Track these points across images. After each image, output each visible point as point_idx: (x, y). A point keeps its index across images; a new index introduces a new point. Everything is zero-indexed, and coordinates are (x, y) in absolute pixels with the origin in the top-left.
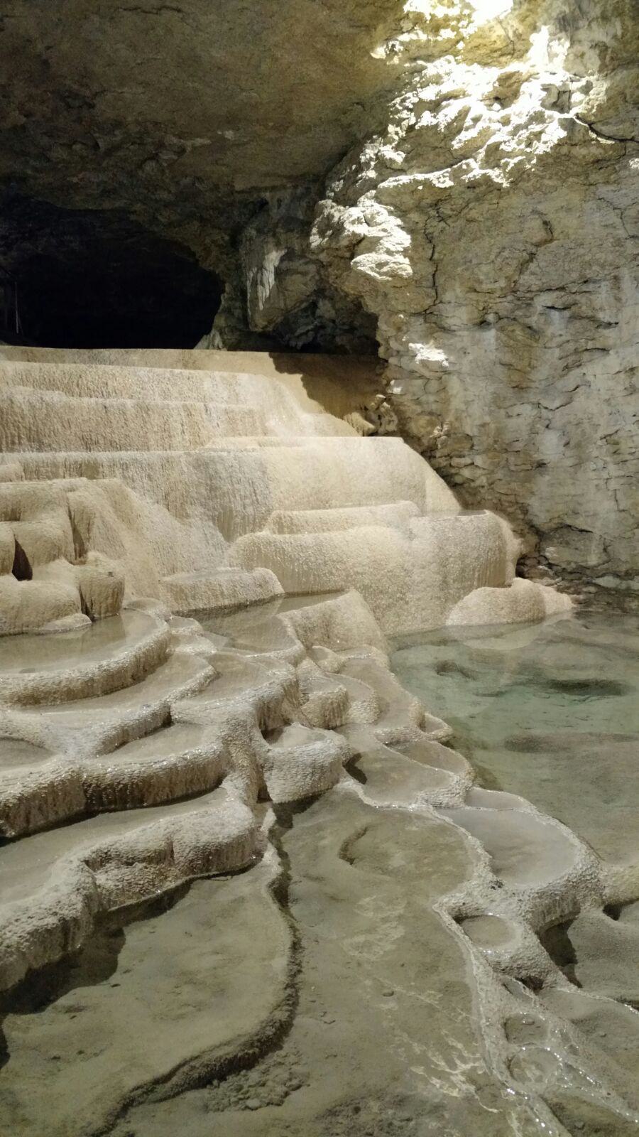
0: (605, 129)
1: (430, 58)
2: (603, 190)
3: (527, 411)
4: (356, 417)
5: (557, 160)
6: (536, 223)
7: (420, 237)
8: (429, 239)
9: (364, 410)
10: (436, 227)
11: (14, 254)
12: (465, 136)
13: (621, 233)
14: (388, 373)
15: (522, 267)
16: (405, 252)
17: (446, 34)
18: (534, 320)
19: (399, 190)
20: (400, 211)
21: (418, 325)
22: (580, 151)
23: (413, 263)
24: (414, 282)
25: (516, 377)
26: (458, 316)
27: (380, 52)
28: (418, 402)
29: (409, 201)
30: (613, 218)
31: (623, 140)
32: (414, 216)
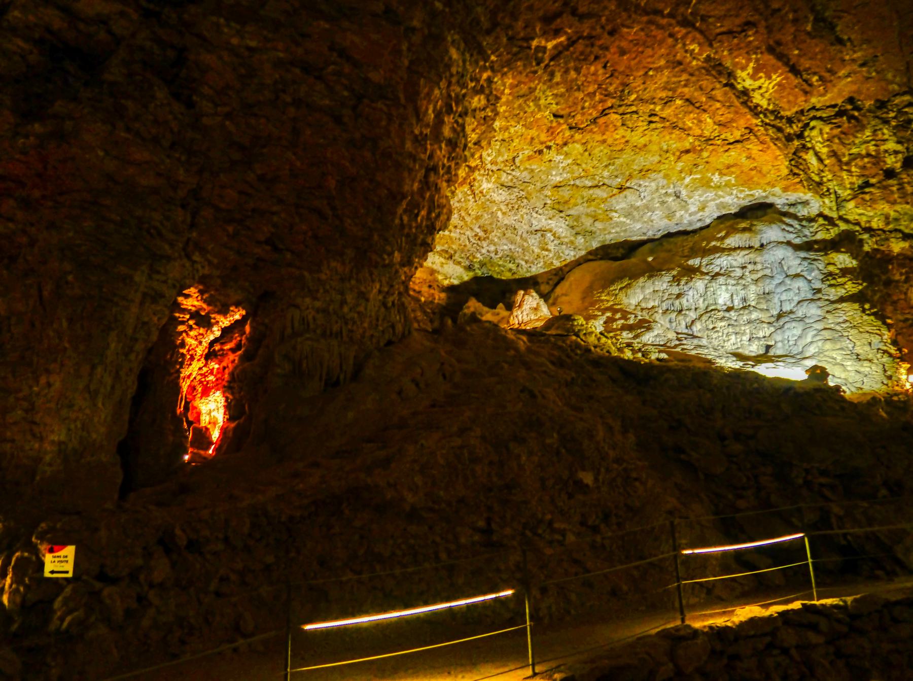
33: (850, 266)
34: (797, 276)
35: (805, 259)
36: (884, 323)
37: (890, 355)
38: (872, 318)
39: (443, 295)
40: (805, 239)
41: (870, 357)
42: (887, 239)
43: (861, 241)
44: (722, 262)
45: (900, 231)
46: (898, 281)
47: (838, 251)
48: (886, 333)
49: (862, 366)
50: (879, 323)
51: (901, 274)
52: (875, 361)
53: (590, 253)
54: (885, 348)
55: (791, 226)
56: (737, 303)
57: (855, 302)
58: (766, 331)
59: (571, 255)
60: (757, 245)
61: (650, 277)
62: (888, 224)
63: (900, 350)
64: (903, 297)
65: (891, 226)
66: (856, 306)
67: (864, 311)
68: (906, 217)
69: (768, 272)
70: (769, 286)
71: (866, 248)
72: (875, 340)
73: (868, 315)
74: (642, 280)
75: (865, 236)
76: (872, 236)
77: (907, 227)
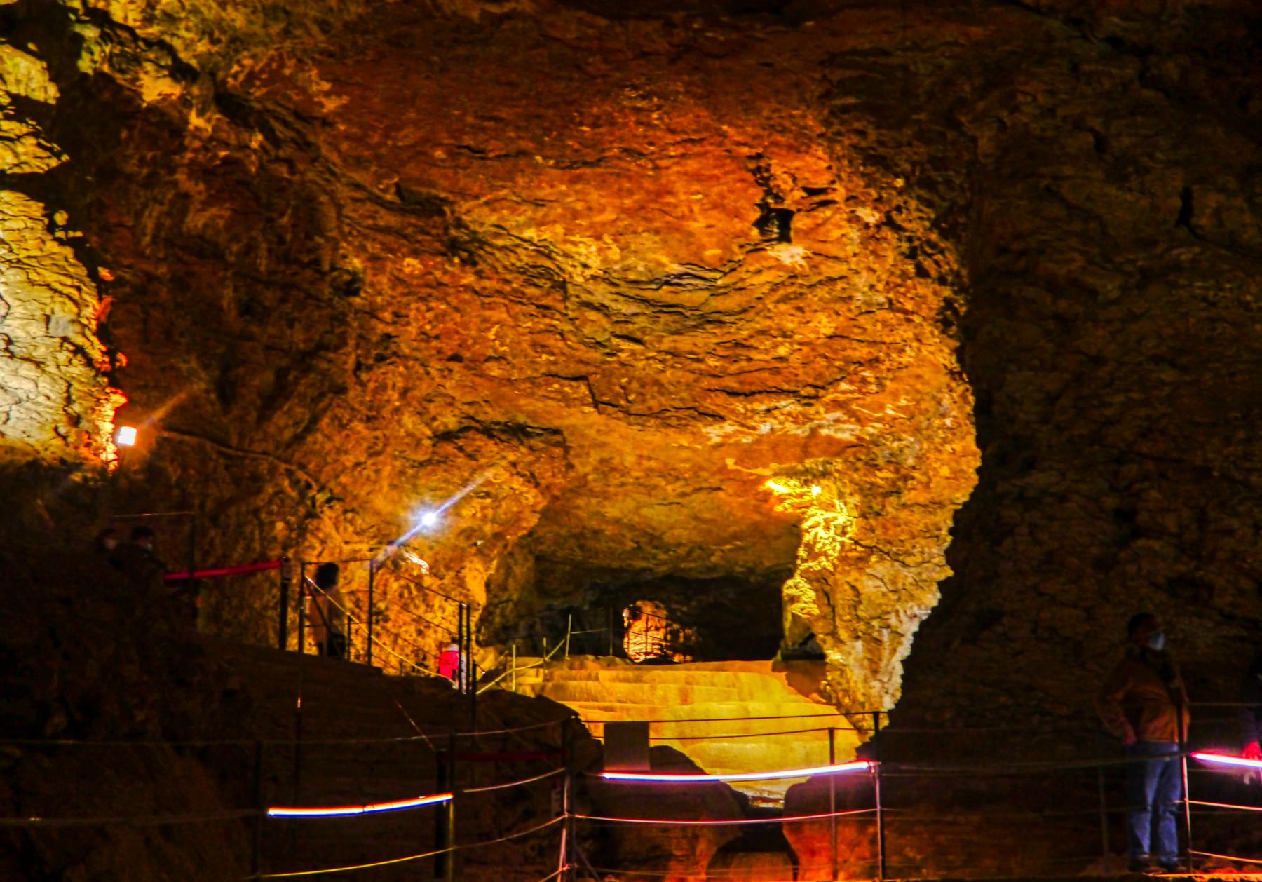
0: (863, 543)
1: (807, 507)
2: (868, 571)
3: (876, 684)
4: (815, 696)
5: (843, 559)
6: (847, 587)
7: (821, 594)
8: (827, 595)
9: (822, 693)
10: (827, 588)
11: (693, 603)
12: (819, 546)
13: (884, 589)
14: (828, 667)
15: (855, 608)
16: (814, 602)
17: (806, 498)
18: (875, 634)
19: (807, 571)
20: (809, 581)
21: (829, 639)
22: (850, 554)
23: (819, 607)
24: (823, 617)
25: (874, 666)
26: (843, 634)
27: (779, 508)
28: (839, 684)
29: (812, 577)
30: (879, 583)
31: (871, 548)
32: (816, 584)
33: (39, 96)
36: (93, 275)
37: (89, 362)
38: (68, 251)
41: (39, 353)
42: (137, 60)
43: (80, 39)
45: (170, 50)
46: (130, 178)
47: (20, 46)
48: (94, 302)
49: (15, 373)
50: (82, 271)
51: (142, 161)
52: (52, 369)
54: (80, 340)
57: (34, 195)
62: (148, 20)
63: (110, 353)
64: (129, 221)
65: (154, 30)
66: (36, 208)
67: (51, 228)
68: (193, 20)
71: (85, 65)
72: (63, 312)
73: (61, 242)
75: (90, 32)
76: (105, 38)
77: (188, 45)
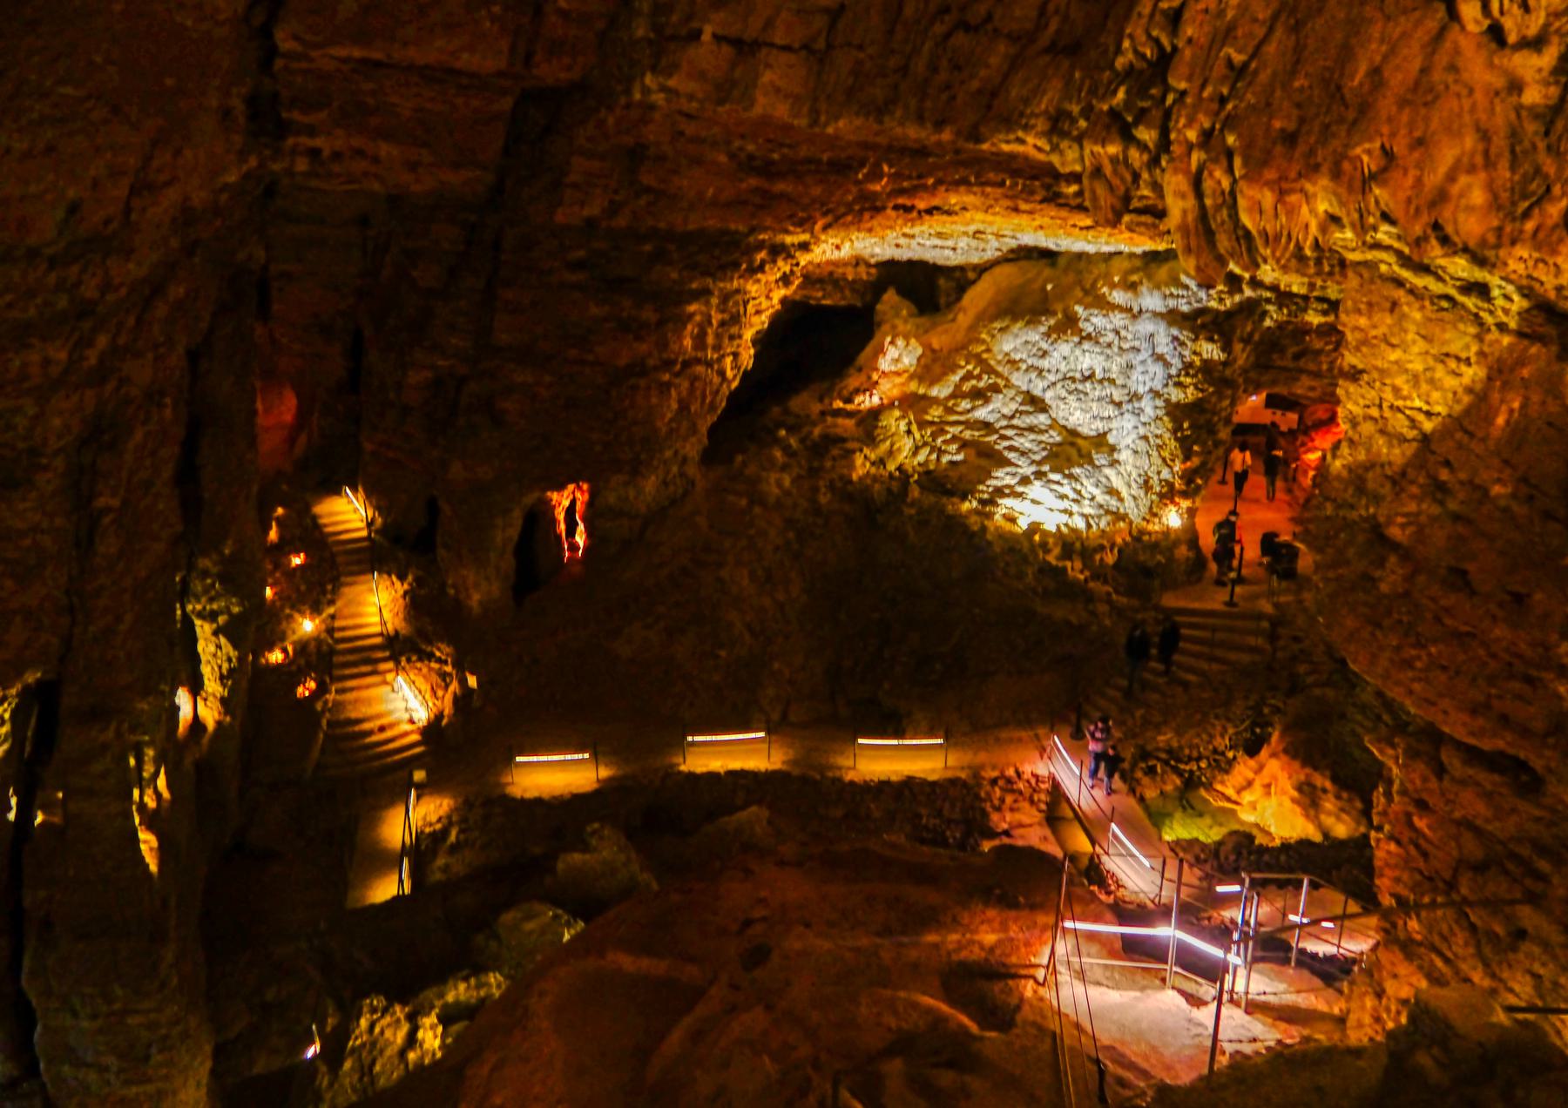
34: (1160, 358)
35: (1175, 338)
39: (873, 271)
40: (1196, 305)
42: (1305, 310)
43: (1265, 313)
44: (1095, 321)
46: (1319, 352)
47: (1211, 340)
53: (1012, 251)
55: (1187, 287)
56: (1099, 375)
58: (1110, 411)
59: (990, 254)
60: (1136, 309)
61: (1028, 323)
65: (1315, 294)
69: (1137, 344)
70: (1136, 359)
74: (1020, 324)
